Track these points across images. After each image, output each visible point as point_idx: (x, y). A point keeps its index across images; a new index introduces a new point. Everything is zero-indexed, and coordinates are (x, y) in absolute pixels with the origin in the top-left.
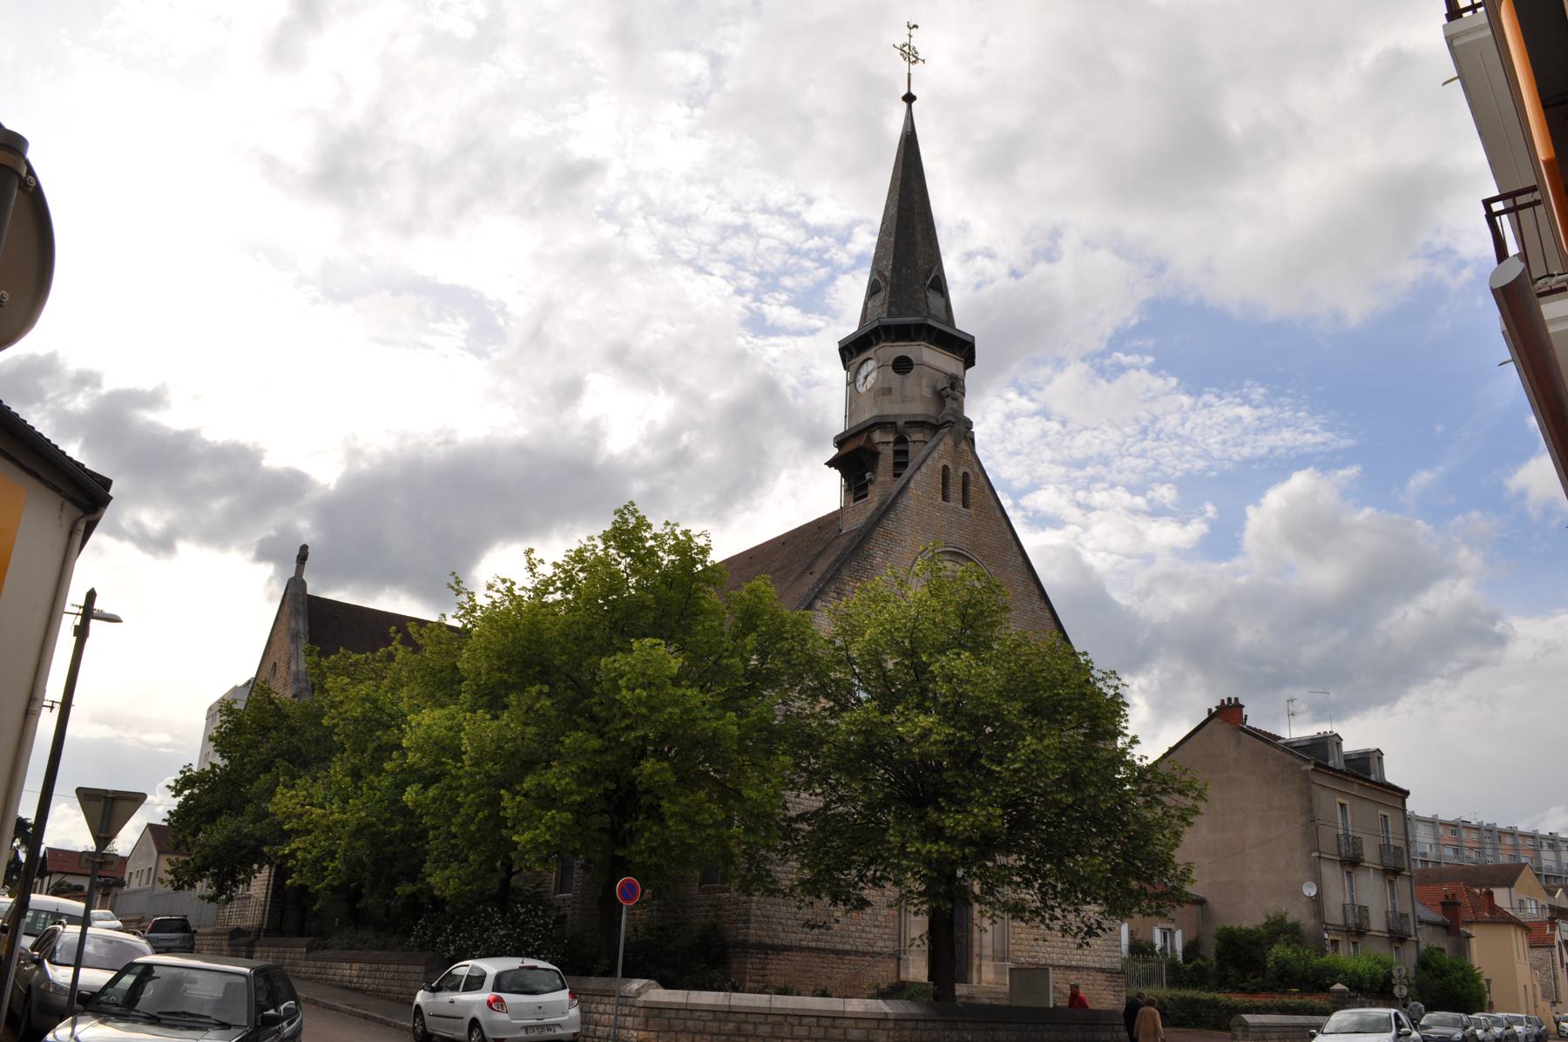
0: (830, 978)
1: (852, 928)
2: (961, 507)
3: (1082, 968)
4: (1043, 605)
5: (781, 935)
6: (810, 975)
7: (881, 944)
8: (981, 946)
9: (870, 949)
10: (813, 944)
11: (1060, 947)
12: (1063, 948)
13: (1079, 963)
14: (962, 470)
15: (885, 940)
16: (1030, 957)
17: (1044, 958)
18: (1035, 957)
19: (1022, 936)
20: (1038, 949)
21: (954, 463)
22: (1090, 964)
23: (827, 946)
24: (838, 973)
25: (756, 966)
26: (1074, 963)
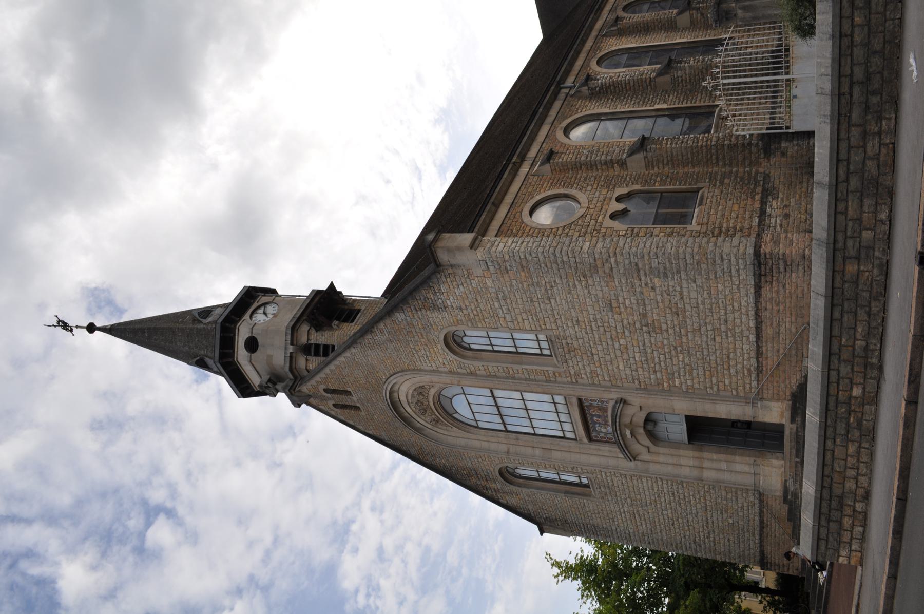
5: (752, 551)
10: (757, 537)
11: (735, 340)
12: (734, 336)
16: (750, 375)
17: (749, 359)
18: (749, 370)
19: (727, 382)
20: (739, 366)
22: (752, 300)
26: (752, 323)
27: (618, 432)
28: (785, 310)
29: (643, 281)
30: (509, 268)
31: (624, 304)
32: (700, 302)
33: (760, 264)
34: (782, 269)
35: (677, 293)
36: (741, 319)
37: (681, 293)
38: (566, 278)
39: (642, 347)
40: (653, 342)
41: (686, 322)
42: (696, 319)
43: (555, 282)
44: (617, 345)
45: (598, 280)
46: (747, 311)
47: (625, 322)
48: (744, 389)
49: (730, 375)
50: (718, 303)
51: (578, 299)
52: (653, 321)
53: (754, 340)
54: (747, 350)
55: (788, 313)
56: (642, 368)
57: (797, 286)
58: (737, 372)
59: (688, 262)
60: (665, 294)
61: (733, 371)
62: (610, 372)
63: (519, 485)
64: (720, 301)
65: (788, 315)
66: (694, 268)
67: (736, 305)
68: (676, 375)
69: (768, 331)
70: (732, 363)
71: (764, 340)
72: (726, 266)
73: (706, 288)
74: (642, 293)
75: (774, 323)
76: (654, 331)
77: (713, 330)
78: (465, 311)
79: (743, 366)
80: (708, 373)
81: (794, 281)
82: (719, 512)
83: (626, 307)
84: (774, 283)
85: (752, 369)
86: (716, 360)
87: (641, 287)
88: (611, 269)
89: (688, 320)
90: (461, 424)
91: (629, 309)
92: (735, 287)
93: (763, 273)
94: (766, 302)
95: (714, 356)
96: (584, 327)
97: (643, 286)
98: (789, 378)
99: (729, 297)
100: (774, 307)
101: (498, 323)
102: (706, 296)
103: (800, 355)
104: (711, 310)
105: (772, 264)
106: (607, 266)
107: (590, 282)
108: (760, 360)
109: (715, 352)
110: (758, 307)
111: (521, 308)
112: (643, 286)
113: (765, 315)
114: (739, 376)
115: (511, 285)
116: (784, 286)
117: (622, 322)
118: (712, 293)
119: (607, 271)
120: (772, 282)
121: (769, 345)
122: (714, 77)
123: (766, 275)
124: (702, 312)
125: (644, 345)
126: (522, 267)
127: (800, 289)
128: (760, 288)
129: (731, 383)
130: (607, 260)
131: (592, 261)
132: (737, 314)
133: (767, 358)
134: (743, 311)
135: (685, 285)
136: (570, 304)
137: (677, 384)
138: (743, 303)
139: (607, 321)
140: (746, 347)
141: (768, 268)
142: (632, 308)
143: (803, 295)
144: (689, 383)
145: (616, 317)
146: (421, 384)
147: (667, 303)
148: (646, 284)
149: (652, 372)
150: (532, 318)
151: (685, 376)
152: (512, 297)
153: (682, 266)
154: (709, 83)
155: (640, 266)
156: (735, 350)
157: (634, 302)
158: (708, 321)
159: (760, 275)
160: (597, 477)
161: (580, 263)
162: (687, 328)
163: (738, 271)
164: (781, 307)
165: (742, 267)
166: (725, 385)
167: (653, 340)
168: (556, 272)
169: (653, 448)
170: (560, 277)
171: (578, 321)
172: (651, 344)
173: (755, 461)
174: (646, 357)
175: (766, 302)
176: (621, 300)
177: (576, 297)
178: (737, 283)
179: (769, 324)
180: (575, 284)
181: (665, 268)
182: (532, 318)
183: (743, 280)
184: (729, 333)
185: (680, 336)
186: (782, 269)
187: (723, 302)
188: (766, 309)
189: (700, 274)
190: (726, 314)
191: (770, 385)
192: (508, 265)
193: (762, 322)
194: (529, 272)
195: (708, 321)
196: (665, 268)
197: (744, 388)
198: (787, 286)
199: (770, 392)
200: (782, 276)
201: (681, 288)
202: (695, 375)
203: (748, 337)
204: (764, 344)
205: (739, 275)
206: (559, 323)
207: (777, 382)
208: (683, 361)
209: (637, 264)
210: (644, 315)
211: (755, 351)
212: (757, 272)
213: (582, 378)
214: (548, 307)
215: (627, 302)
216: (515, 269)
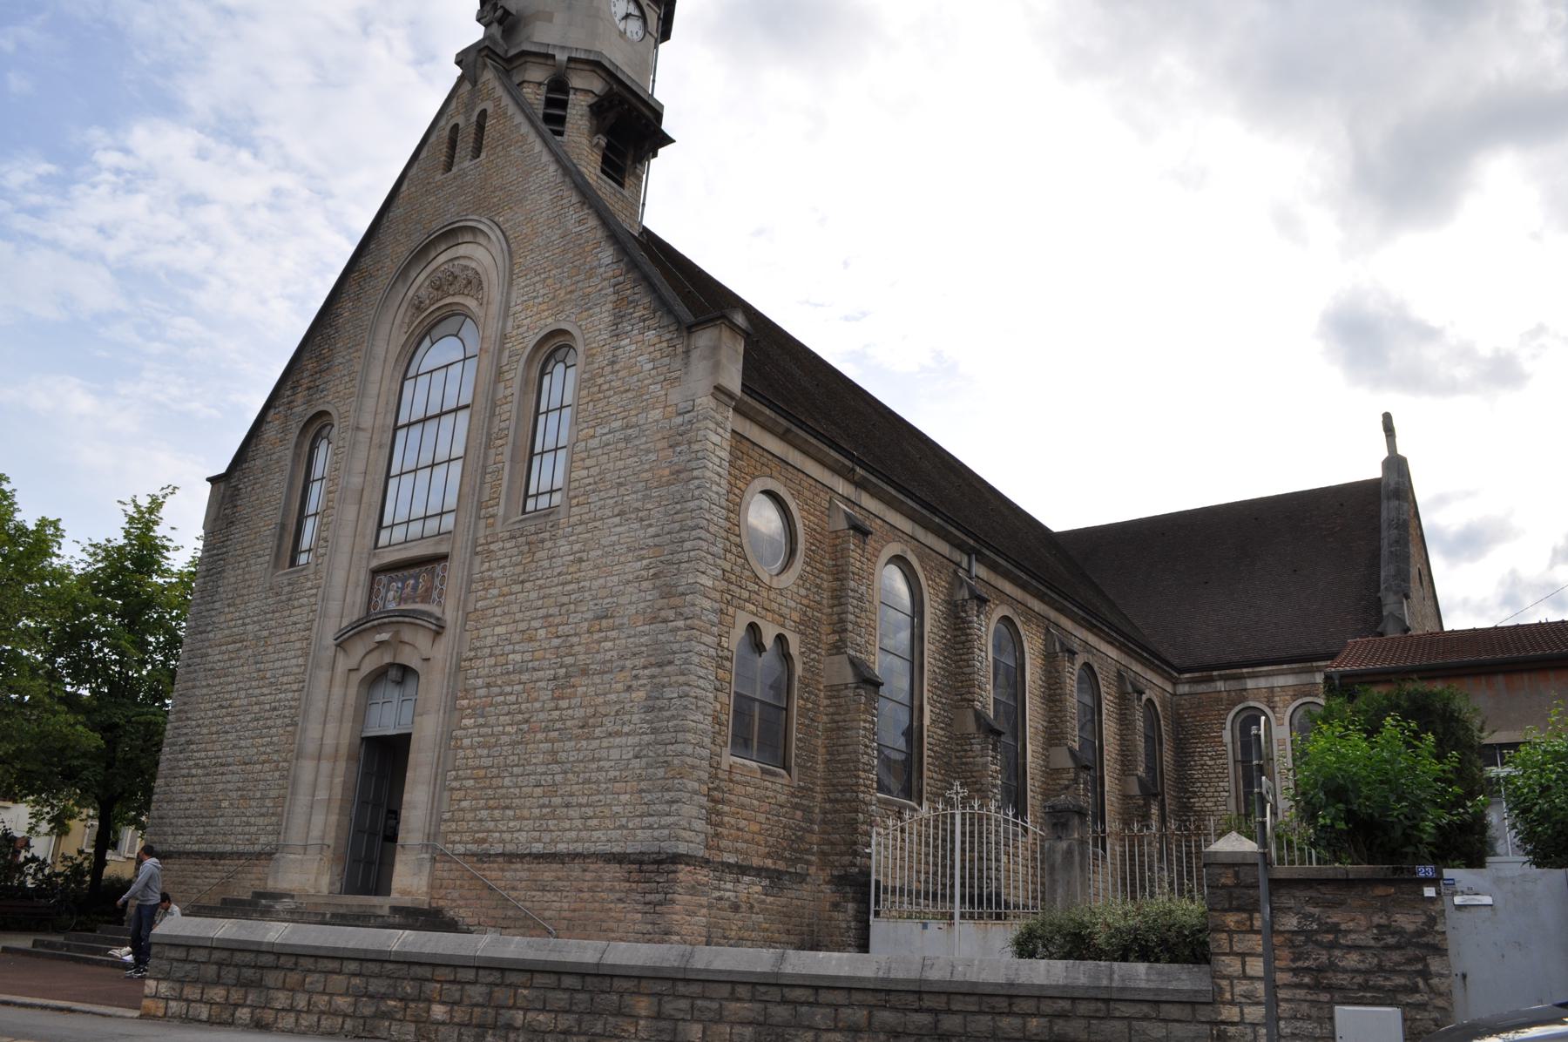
5: (170, 839)
10: (195, 848)
11: (535, 819)
12: (542, 817)
17: (502, 841)
18: (484, 841)
20: (491, 825)
22: (600, 848)
26: (562, 847)
27: (386, 620)
28: (582, 900)
30: (678, 449)
31: (606, 639)
32: (601, 763)
33: (659, 862)
34: (649, 897)
35: (619, 728)
36: (570, 830)
37: (618, 734)
38: (655, 545)
39: (530, 665)
41: (570, 740)
42: (573, 756)
43: (650, 525)
44: (535, 624)
45: (649, 598)
47: (575, 640)
49: (476, 809)
50: (599, 792)
51: (619, 563)
52: (574, 686)
53: (534, 850)
54: (517, 838)
55: (577, 905)
56: (496, 665)
57: (620, 921)
58: (481, 820)
59: (669, 747)
61: (484, 814)
63: (298, 445)
64: (601, 797)
65: (573, 906)
66: (659, 755)
67: (595, 822)
68: (481, 721)
69: (548, 873)
70: (497, 813)
72: (659, 807)
73: (625, 774)
74: (623, 669)
75: (560, 883)
76: (557, 687)
77: (554, 784)
78: (608, 369)
79: (491, 831)
80: (482, 773)
81: (629, 916)
82: (240, 785)
83: (600, 642)
84: (627, 884)
85: (485, 846)
86: (502, 787)
87: (633, 669)
88: (665, 621)
89: (573, 743)
90: (412, 349)
91: (597, 647)
92: (624, 821)
93: (645, 867)
95: (510, 784)
96: (571, 570)
97: (634, 672)
98: (467, 906)
99: (607, 812)
100: (586, 884)
101: (585, 425)
102: (612, 774)
104: (588, 781)
105: (658, 883)
106: (671, 614)
107: (645, 585)
108: (500, 859)
109: (516, 786)
110: (588, 858)
112: (634, 672)
113: (576, 869)
114: (474, 823)
115: (648, 451)
116: (620, 900)
117: (576, 635)
118: (616, 784)
119: (663, 614)
120: (628, 881)
121: (524, 875)
122: (965, 801)
123: (641, 871)
124: (585, 767)
125: (534, 669)
126: (678, 472)
127: (614, 925)
128: (620, 863)
129: (462, 810)
130: (681, 614)
131: (681, 589)
132: (578, 823)
133: (503, 870)
134: (584, 834)
135: (631, 740)
136: (610, 549)
137: (466, 722)
138: (596, 834)
139: (579, 609)
141: (652, 875)
142: (598, 652)
143: (605, 931)
145: (585, 625)
146: (485, 285)
147: (602, 710)
148: (636, 677)
149: (487, 680)
150: (590, 484)
152: (629, 452)
153: (664, 736)
154: (957, 793)
155: (668, 669)
156: (518, 819)
157: (608, 656)
158: (570, 776)
159: (641, 863)
160: (308, 580)
161: (678, 569)
162: (559, 741)
163: (650, 827)
164: (586, 895)
165: (656, 833)
166: (460, 800)
167: (542, 684)
168: (667, 528)
169: (356, 678)
170: (658, 536)
171: (581, 560)
173: (329, 846)
174: (514, 672)
176: (613, 634)
177: (622, 559)
178: (630, 826)
179: (560, 874)
180: (643, 558)
181: (661, 709)
182: (590, 484)
183: (635, 836)
184: (548, 810)
185: (546, 730)
186: (649, 897)
187: (600, 801)
188: (585, 870)
189: (649, 766)
190: (580, 805)
191: (458, 873)
192: (682, 448)
193: (563, 864)
194: (669, 484)
195: (570, 776)
196: (661, 709)
197: (456, 832)
199: (445, 874)
200: (638, 897)
201: (627, 734)
202: (479, 751)
203: (539, 840)
204: (526, 866)
205: (643, 828)
206: (580, 529)
207: (461, 886)
208: (504, 733)
209: (670, 663)
210: (584, 672)
211: (515, 851)
212: (646, 858)
213: (482, 563)
214: (608, 512)
215: (609, 645)
216: (676, 459)
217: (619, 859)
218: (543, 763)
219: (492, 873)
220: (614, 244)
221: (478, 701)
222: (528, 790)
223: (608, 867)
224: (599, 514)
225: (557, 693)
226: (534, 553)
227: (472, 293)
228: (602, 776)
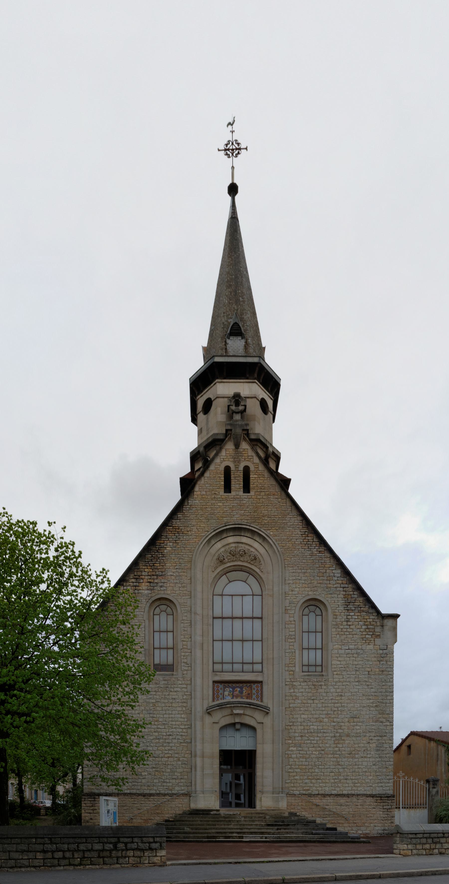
0: (139, 809)
1: (155, 781)
2: (241, 493)
3: (353, 795)
4: (322, 549)
6: (125, 808)
7: (177, 788)
8: (263, 786)
9: (170, 792)
13: (350, 792)
14: (241, 468)
15: (181, 786)
16: (305, 790)
17: (319, 791)
18: (308, 790)
19: (296, 777)
20: (312, 785)
21: (234, 462)
22: (361, 792)
23: (138, 792)
24: (146, 806)
25: (88, 805)
26: (345, 792)
28: (358, 808)
29: (373, 738)
30: (382, 663)
31: (357, 725)
33: (388, 797)
37: (365, 757)
39: (322, 731)
40: (327, 738)
41: (344, 758)
43: (372, 688)
44: (324, 716)
46: (354, 790)
47: (343, 724)
48: (292, 787)
50: (359, 775)
51: (359, 699)
53: (333, 793)
55: (356, 810)
56: (304, 729)
58: (306, 783)
60: (364, 749)
61: (307, 781)
62: (298, 709)
67: (358, 785)
68: (300, 749)
69: (342, 800)
70: (313, 781)
71: (335, 798)
72: (385, 781)
73: (370, 770)
74: (365, 736)
77: (339, 772)
78: (345, 623)
80: (304, 767)
81: (378, 813)
82: (154, 766)
85: (309, 792)
86: (315, 772)
88: (382, 722)
89: (346, 759)
91: (353, 728)
92: (371, 785)
93: (383, 798)
94: (363, 800)
96: (337, 699)
97: (370, 738)
99: (363, 781)
101: (336, 643)
102: (364, 770)
103: (324, 816)
104: (355, 772)
106: (384, 720)
107: (372, 709)
108: (320, 796)
109: (321, 772)
111: (350, 662)
112: (370, 738)
113: (354, 799)
115: (368, 661)
117: (342, 722)
119: (381, 719)
121: (332, 801)
125: (324, 732)
126: (383, 671)
127: (372, 815)
128: (373, 797)
131: (387, 712)
133: (321, 799)
134: (354, 788)
135: (371, 760)
136: (355, 694)
138: (359, 789)
140: (327, 789)
142: (353, 729)
144: (293, 756)
145: (347, 720)
148: (371, 739)
149: (301, 734)
151: (300, 754)
152: (359, 659)
153: (385, 759)
155: (384, 738)
157: (358, 731)
158: (346, 770)
159: (381, 797)
160: (178, 680)
163: (382, 786)
164: (359, 807)
165: (384, 788)
166: (294, 776)
167: (329, 738)
168: (379, 690)
171: (341, 696)
172: (326, 737)
173: (216, 791)
174: (314, 732)
175: (363, 800)
176: (360, 724)
177: (361, 698)
178: (373, 786)
179: (348, 801)
180: (370, 699)
183: (376, 789)
185: (333, 754)
186: (385, 807)
189: (379, 768)
190: (352, 779)
194: (379, 674)
195: (346, 770)
196: (383, 751)
197: (294, 787)
198: (374, 810)
201: (369, 758)
202: (301, 759)
203: (335, 790)
206: (339, 684)
208: (312, 754)
209: (385, 736)
210: (348, 735)
212: (383, 796)
213: (290, 689)
214: (352, 680)
215: (358, 727)
216: (381, 666)
217: (372, 796)
218: (333, 765)
219: (316, 800)
220: (340, 568)
221: (297, 741)
222: (328, 774)
223: (367, 798)
224: (348, 680)
225: (336, 742)
226: (317, 689)
227: (256, 564)
228: (360, 770)
